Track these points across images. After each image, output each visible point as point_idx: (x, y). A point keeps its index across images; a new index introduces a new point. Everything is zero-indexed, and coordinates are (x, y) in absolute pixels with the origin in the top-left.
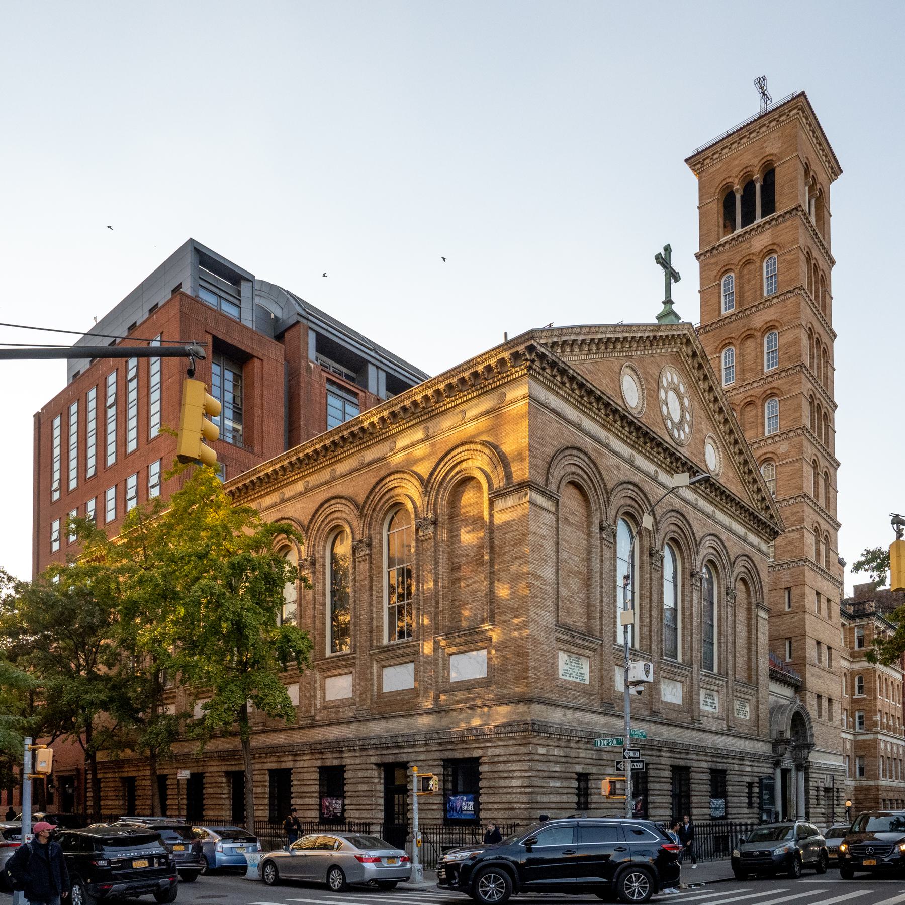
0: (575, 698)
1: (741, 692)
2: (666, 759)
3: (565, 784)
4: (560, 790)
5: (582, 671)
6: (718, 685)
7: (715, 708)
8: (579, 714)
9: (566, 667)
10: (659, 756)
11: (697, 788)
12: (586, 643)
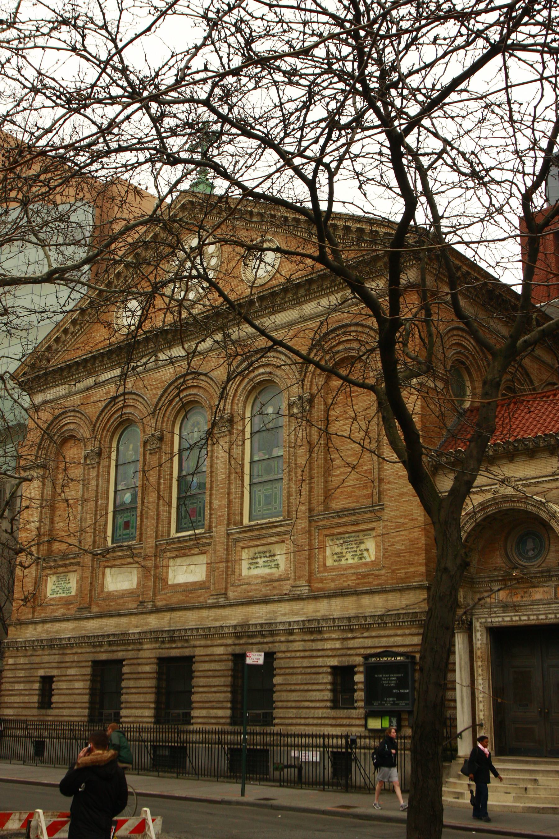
0: (53, 611)
1: (340, 525)
2: (150, 651)
3: (28, 686)
4: (23, 692)
5: (69, 585)
6: (277, 534)
7: (277, 566)
8: (48, 626)
9: (54, 587)
10: (139, 650)
11: (202, 681)
12: (68, 562)
